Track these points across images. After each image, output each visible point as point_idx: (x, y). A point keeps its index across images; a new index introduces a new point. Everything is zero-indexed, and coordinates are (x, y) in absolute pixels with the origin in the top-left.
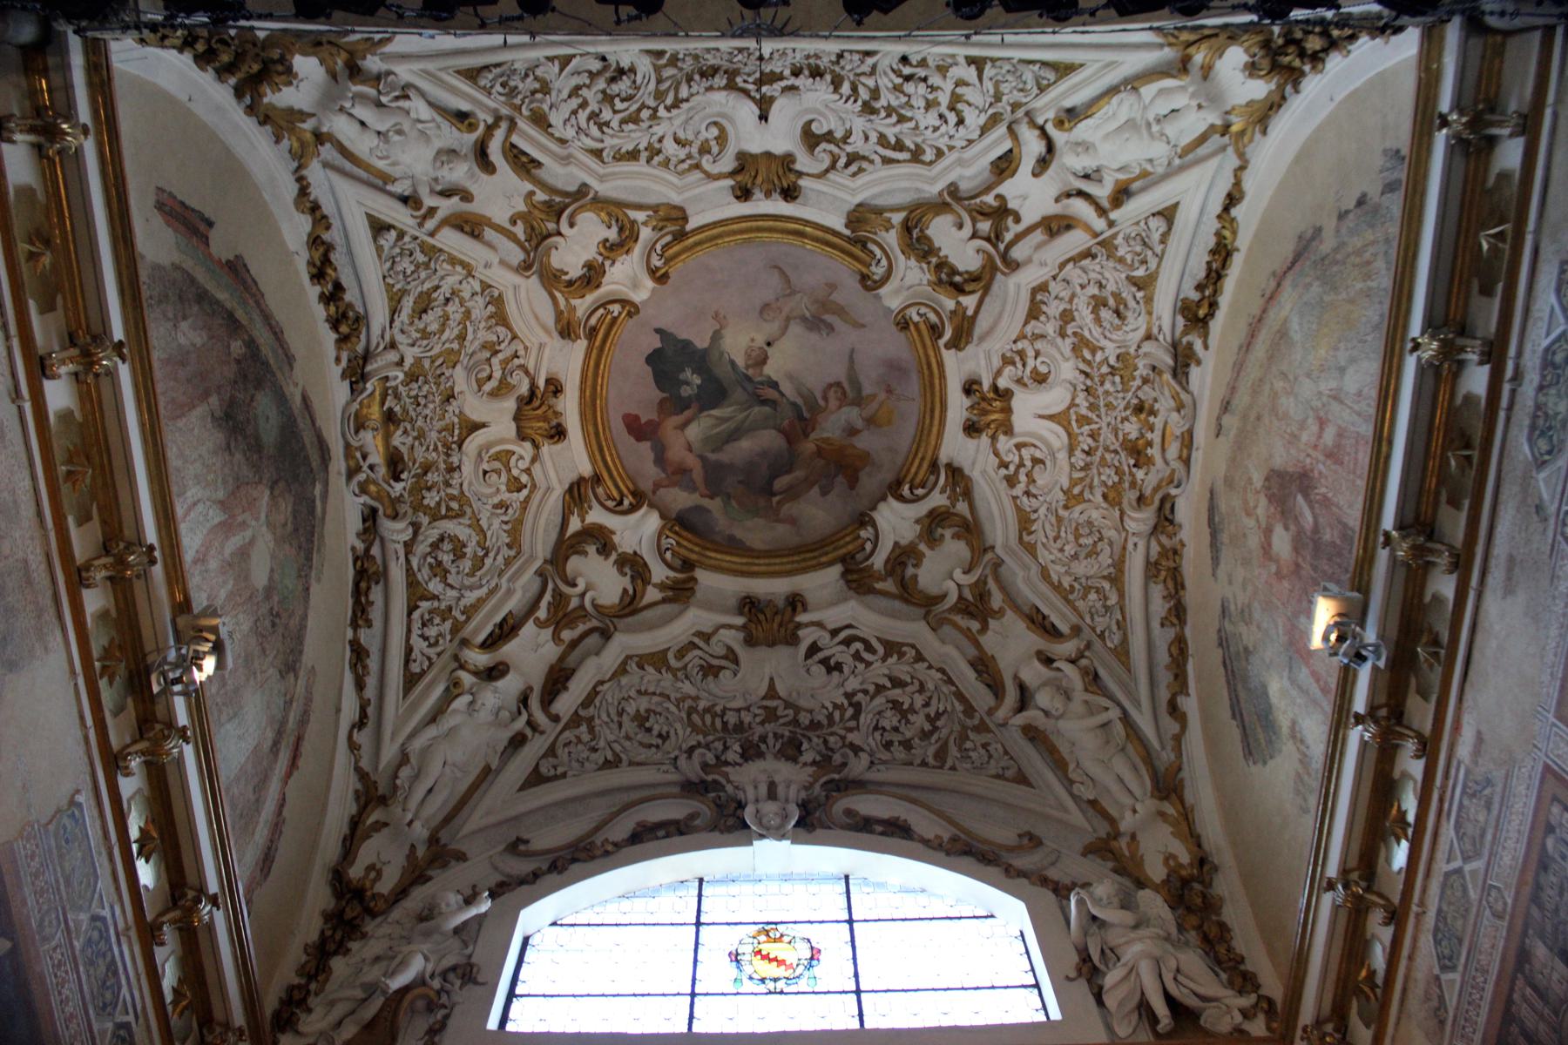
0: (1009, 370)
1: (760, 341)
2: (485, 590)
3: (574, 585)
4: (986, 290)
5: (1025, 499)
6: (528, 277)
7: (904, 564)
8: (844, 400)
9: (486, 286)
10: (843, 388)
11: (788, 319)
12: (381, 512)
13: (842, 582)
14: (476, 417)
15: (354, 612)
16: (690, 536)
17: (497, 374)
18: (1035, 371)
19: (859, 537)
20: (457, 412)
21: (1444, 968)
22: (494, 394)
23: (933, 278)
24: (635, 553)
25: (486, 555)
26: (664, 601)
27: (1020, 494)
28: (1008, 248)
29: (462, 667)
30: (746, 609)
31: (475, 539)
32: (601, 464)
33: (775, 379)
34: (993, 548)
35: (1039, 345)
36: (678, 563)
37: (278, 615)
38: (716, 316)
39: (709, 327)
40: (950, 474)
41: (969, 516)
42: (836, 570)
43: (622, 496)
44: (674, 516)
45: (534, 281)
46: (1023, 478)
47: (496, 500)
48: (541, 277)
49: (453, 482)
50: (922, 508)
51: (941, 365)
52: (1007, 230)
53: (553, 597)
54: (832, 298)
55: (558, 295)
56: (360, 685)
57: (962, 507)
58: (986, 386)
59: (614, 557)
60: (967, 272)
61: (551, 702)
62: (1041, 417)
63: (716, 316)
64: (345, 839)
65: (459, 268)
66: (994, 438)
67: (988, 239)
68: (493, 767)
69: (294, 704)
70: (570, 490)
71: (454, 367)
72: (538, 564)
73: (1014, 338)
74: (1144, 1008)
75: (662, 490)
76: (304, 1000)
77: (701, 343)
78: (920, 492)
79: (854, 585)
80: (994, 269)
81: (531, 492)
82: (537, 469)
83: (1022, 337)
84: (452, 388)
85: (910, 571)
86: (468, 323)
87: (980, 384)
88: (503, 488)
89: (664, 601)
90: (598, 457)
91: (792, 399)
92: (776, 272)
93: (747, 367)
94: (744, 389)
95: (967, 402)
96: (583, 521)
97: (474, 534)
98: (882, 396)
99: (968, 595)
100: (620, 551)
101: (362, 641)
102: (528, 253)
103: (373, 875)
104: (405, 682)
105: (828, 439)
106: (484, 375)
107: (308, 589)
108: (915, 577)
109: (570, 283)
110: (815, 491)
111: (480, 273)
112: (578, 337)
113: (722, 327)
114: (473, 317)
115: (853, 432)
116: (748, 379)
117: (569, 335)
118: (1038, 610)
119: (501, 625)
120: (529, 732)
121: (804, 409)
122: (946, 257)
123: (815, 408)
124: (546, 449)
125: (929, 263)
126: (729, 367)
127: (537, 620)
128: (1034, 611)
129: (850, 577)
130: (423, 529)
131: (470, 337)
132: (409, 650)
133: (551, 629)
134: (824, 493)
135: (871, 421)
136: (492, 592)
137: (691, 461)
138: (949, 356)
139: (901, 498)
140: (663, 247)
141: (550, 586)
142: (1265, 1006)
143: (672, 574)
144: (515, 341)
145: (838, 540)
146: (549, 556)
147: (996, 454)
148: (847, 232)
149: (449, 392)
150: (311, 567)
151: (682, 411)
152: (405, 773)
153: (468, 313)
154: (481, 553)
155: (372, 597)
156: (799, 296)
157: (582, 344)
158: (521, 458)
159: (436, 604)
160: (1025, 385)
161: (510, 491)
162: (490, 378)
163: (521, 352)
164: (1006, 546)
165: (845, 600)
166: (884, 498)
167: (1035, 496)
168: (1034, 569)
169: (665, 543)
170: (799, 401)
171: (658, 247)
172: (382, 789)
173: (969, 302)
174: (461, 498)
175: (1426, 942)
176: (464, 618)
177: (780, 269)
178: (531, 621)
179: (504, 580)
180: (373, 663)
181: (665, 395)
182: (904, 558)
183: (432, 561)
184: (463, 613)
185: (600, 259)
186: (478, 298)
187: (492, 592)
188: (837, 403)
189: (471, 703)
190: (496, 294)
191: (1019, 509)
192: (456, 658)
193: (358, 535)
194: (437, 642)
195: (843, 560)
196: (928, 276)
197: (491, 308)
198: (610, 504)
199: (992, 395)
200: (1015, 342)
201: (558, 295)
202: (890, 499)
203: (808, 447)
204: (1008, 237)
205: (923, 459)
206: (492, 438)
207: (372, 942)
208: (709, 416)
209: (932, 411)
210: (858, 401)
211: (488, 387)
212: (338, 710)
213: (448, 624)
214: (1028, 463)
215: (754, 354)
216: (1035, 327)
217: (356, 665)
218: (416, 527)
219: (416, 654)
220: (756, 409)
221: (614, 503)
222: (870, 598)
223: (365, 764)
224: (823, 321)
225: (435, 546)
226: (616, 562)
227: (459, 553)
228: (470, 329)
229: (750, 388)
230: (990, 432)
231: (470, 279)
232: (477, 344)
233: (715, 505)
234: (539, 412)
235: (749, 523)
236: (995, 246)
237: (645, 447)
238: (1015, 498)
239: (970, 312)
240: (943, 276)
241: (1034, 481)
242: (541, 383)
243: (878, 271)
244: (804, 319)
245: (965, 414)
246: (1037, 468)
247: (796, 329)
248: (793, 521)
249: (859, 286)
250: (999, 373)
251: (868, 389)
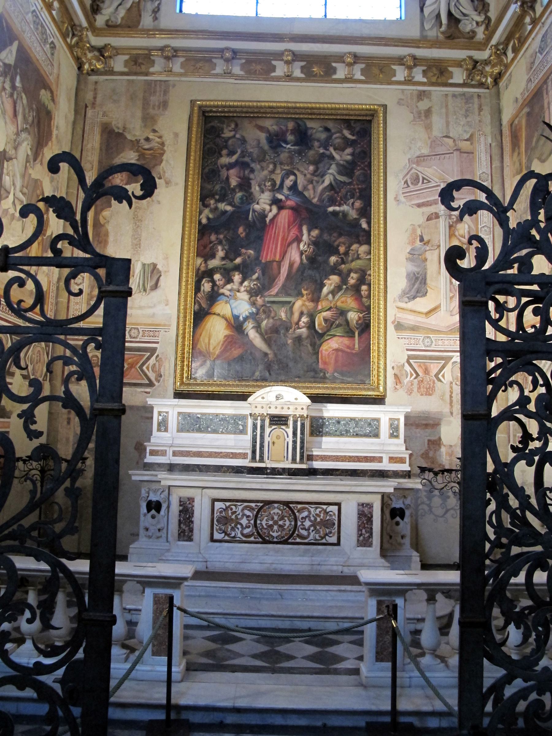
21: (539, 51)
74: (438, 16)
142: (487, 22)
175: (540, 36)
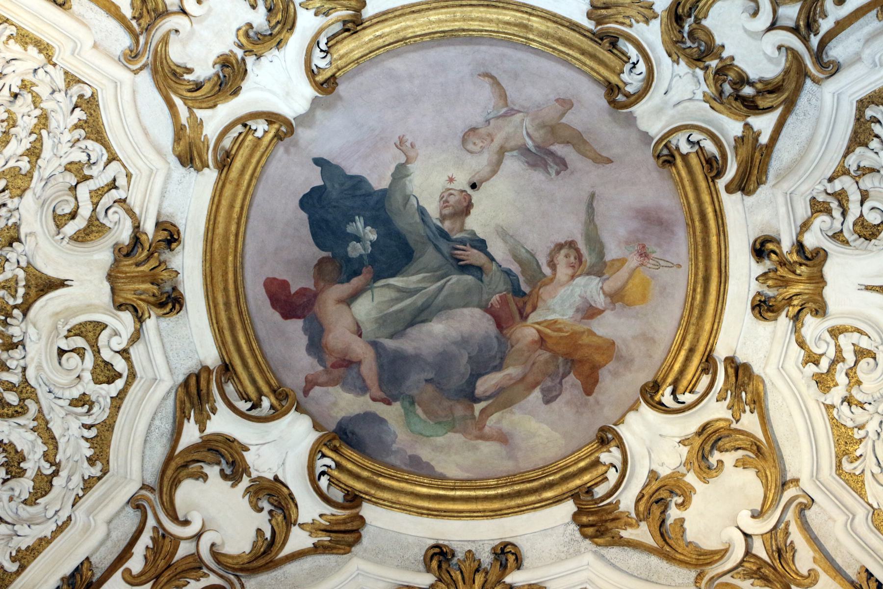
0: (821, 221)
1: (462, 182)
3: (186, 523)
4: (790, 105)
5: (845, 407)
6: (136, 72)
7: (663, 504)
8: (578, 266)
9: (71, 80)
10: (577, 250)
11: (502, 152)
13: (574, 527)
14: (52, 271)
16: (355, 456)
17: (85, 211)
18: (861, 221)
19: (597, 463)
20: (23, 264)
22: (82, 237)
23: (711, 91)
24: (276, 479)
25: (56, 473)
26: (317, 549)
27: (837, 401)
28: (823, 44)
30: (434, 564)
31: (41, 448)
32: (232, 348)
33: (481, 236)
34: (796, 481)
35: (867, 183)
36: (338, 495)
38: (401, 144)
39: (391, 159)
40: (731, 371)
41: (760, 435)
42: (569, 507)
43: (260, 394)
44: (333, 426)
45: (145, 77)
46: (841, 379)
47: (76, 393)
48: (155, 72)
49: (11, 364)
50: (691, 423)
51: (719, 215)
52: (825, 16)
53: (153, 539)
54: (564, 120)
55: (178, 101)
57: (750, 422)
58: (786, 245)
59: (245, 482)
60: (761, 81)
62: (868, 288)
63: (401, 144)
65: (32, 50)
66: (796, 318)
67: (795, 30)
70: (186, 384)
71: (21, 196)
72: (132, 488)
73: (829, 174)
75: (317, 388)
77: (379, 180)
78: (688, 398)
79: (590, 531)
80: (802, 73)
81: (128, 384)
82: (136, 352)
83: (842, 171)
84: (16, 226)
85: (674, 513)
86: (44, 133)
87: (778, 242)
88: (87, 376)
89: (317, 549)
90: (229, 339)
91: (505, 265)
92: (486, 83)
93: (443, 218)
94: (436, 247)
95: (759, 269)
96: (202, 430)
97: (39, 441)
98: (634, 261)
99: (759, 549)
100: (254, 475)
102: (136, 37)
105: (555, 322)
106: (68, 209)
108: (682, 520)
109: (198, 86)
110: (536, 395)
111: (63, 57)
112: (205, 165)
113: (407, 162)
114: (53, 124)
115: (590, 312)
116: (444, 235)
117: (192, 160)
118: (870, 575)
121: (522, 279)
122: (732, 58)
123: (537, 279)
124: (150, 324)
125: (706, 68)
126: (417, 218)
127: (128, 571)
128: (864, 575)
129: (585, 519)
131: (46, 153)
134: (548, 401)
135: (616, 297)
136: (60, 529)
137: (360, 349)
138: (732, 203)
139: (660, 407)
140: (329, 39)
141: (151, 522)
143: (328, 510)
144: (114, 165)
145: (567, 467)
146: (151, 479)
147: (801, 344)
148: (589, 25)
149: (12, 233)
151: (348, 280)
153: (44, 120)
154: (49, 472)
156: (518, 117)
157: (211, 175)
158: (116, 333)
160: (846, 242)
161: (97, 382)
162: (73, 215)
163: (122, 181)
164: (815, 476)
165: (578, 553)
166: (634, 407)
167: (861, 405)
168: (861, 513)
169: (321, 464)
170: (515, 268)
171: (323, 41)
173: (764, 124)
174: (25, 389)
177: (492, 77)
178: (118, 574)
179: (80, 515)
181: (324, 254)
182: (664, 494)
184: (13, 560)
185: (240, 53)
186: (59, 96)
187: (60, 529)
188: (570, 271)
190: (88, 93)
191: (836, 424)
195: (575, 496)
196: (704, 87)
197: (79, 114)
198: (243, 406)
199: (795, 257)
200: (831, 180)
201: (178, 101)
202: (644, 408)
203: (526, 333)
204: (825, 25)
205: (692, 351)
206: (73, 304)
208: (388, 286)
209: (707, 280)
210: (599, 269)
211: (71, 228)
214: (850, 358)
215: (452, 200)
216: (862, 155)
220: (455, 278)
221: (249, 405)
222: (613, 553)
224: (552, 154)
226: (247, 491)
228: (47, 143)
229: (445, 246)
230: (793, 311)
231: (50, 68)
232: (56, 163)
233: (392, 413)
234: (145, 268)
235: (440, 440)
236: (805, 41)
237: (296, 326)
238: (829, 407)
239: (764, 139)
240: (728, 89)
241: (859, 383)
242: (149, 227)
243: (632, 81)
244: (524, 151)
245: (755, 287)
246: (863, 363)
247: (512, 164)
248: (503, 438)
249: (604, 103)
250: (805, 226)
251: (613, 252)
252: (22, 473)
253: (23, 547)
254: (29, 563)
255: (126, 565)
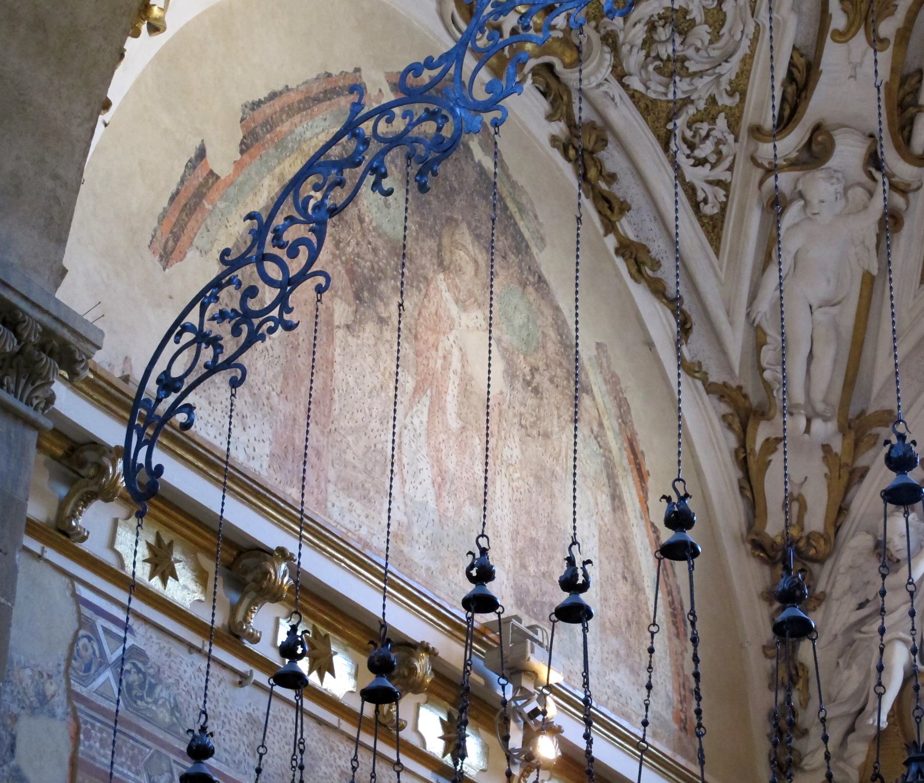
2: (746, 43)
12: (559, 67)
15: (600, 212)
29: (772, 170)
37: (534, 370)
56: (658, 289)
61: (908, 141)
64: (741, 488)
68: (875, 272)
69: (606, 423)
76: (792, 724)
101: (632, 236)
103: (795, 507)
104: (707, 233)
107: (541, 279)
119: (790, 78)
120: (898, 200)
127: (836, 32)
130: (621, 37)
132: (691, 191)
133: (862, 31)
150: (527, 246)
152: (768, 355)
155: (610, 167)
159: (691, 110)
172: (755, 397)
176: (737, 97)
178: (829, 40)
180: (658, 246)
183: (657, 63)
187: (755, 40)
189: (805, 206)
192: (753, 160)
193: (550, 118)
194: (719, 153)
207: (834, 606)
212: (650, 345)
213: (721, 122)
217: (639, 271)
218: (611, 41)
219: (702, 191)
223: (716, 377)
225: (648, 43)
227: (684, 26)
252: (693, 23)
253: (733, 77)
254: (746, 85)
255: (832, 28)
